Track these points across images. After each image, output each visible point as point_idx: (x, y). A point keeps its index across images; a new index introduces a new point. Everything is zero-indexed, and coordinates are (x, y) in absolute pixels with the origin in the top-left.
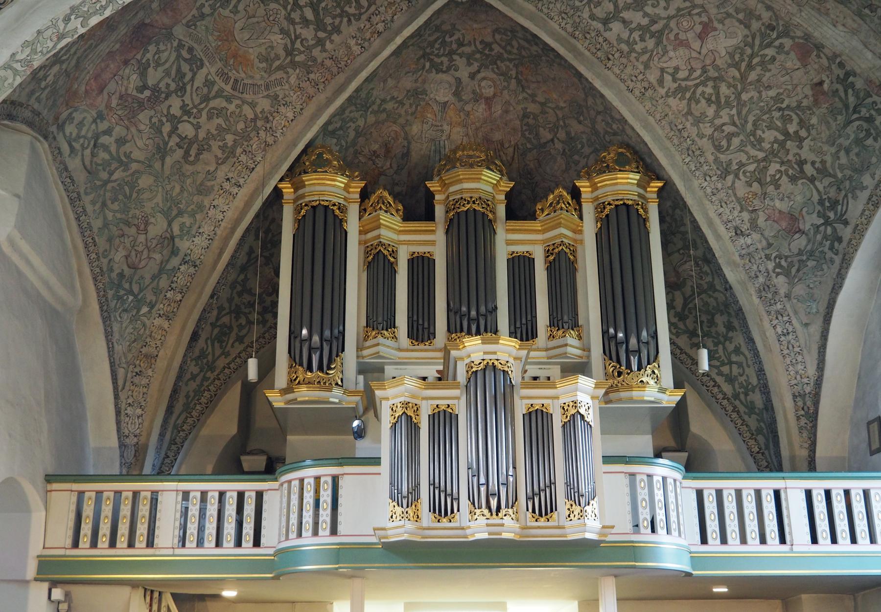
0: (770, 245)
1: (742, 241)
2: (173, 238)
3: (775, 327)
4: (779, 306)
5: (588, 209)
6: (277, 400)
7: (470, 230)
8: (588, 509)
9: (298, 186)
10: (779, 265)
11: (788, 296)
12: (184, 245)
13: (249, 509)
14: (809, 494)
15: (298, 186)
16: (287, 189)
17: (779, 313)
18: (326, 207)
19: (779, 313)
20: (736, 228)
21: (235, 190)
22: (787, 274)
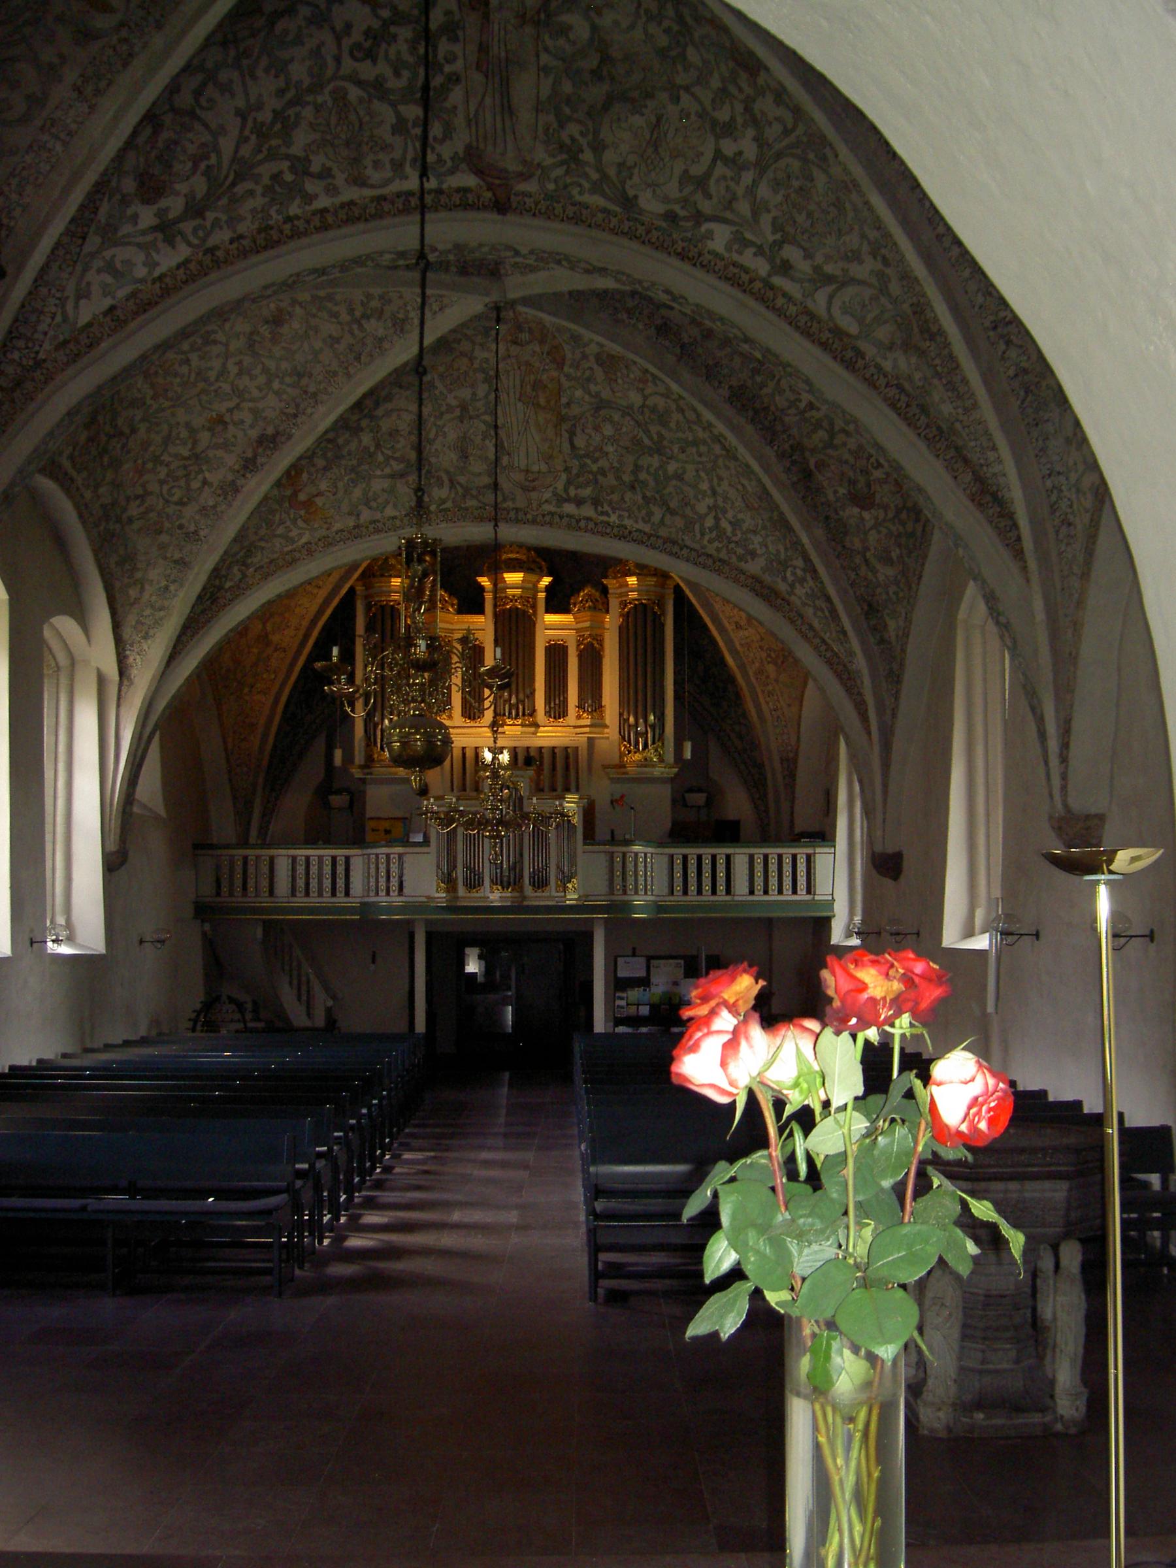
0: (762, 639)
1: (741, 633)
2: (267, 635)
3: (767, 703)
4: (770, 688)
5: (614, 603)
6: (357, 773)
7: (515, 626)
8: (569, 885)
9: (368, 587)
10: (769, 656)
11: (776, 681)
12: (275, 638)
13: (341, 870)
14: (751, 858)
15: (368, 587)
16: (359, 588)
17: (770, 694)
18: (392, 607)
19: (770, 694)
20: (737, 623)
21: (315, 591)
22: (775, 664)
